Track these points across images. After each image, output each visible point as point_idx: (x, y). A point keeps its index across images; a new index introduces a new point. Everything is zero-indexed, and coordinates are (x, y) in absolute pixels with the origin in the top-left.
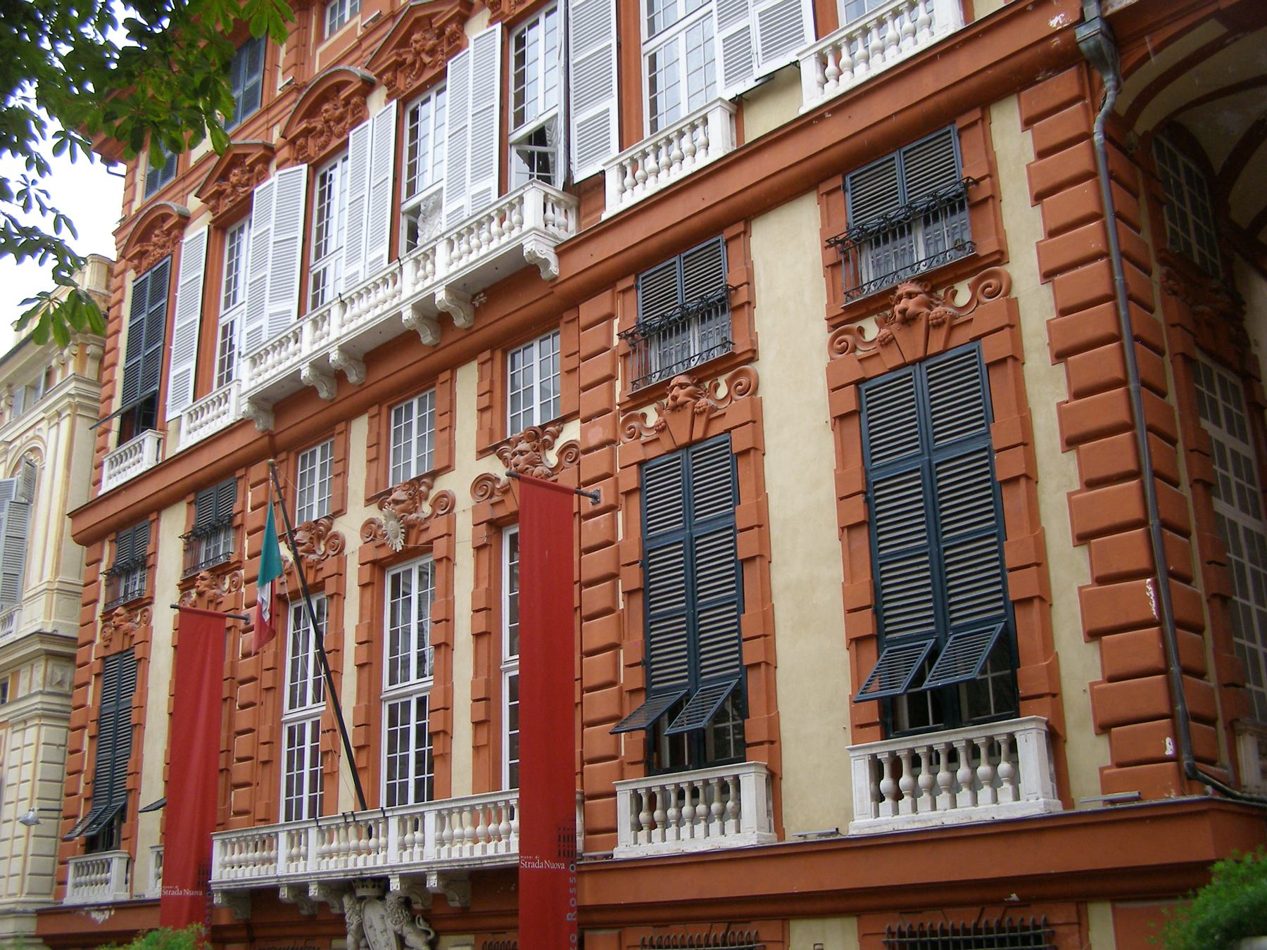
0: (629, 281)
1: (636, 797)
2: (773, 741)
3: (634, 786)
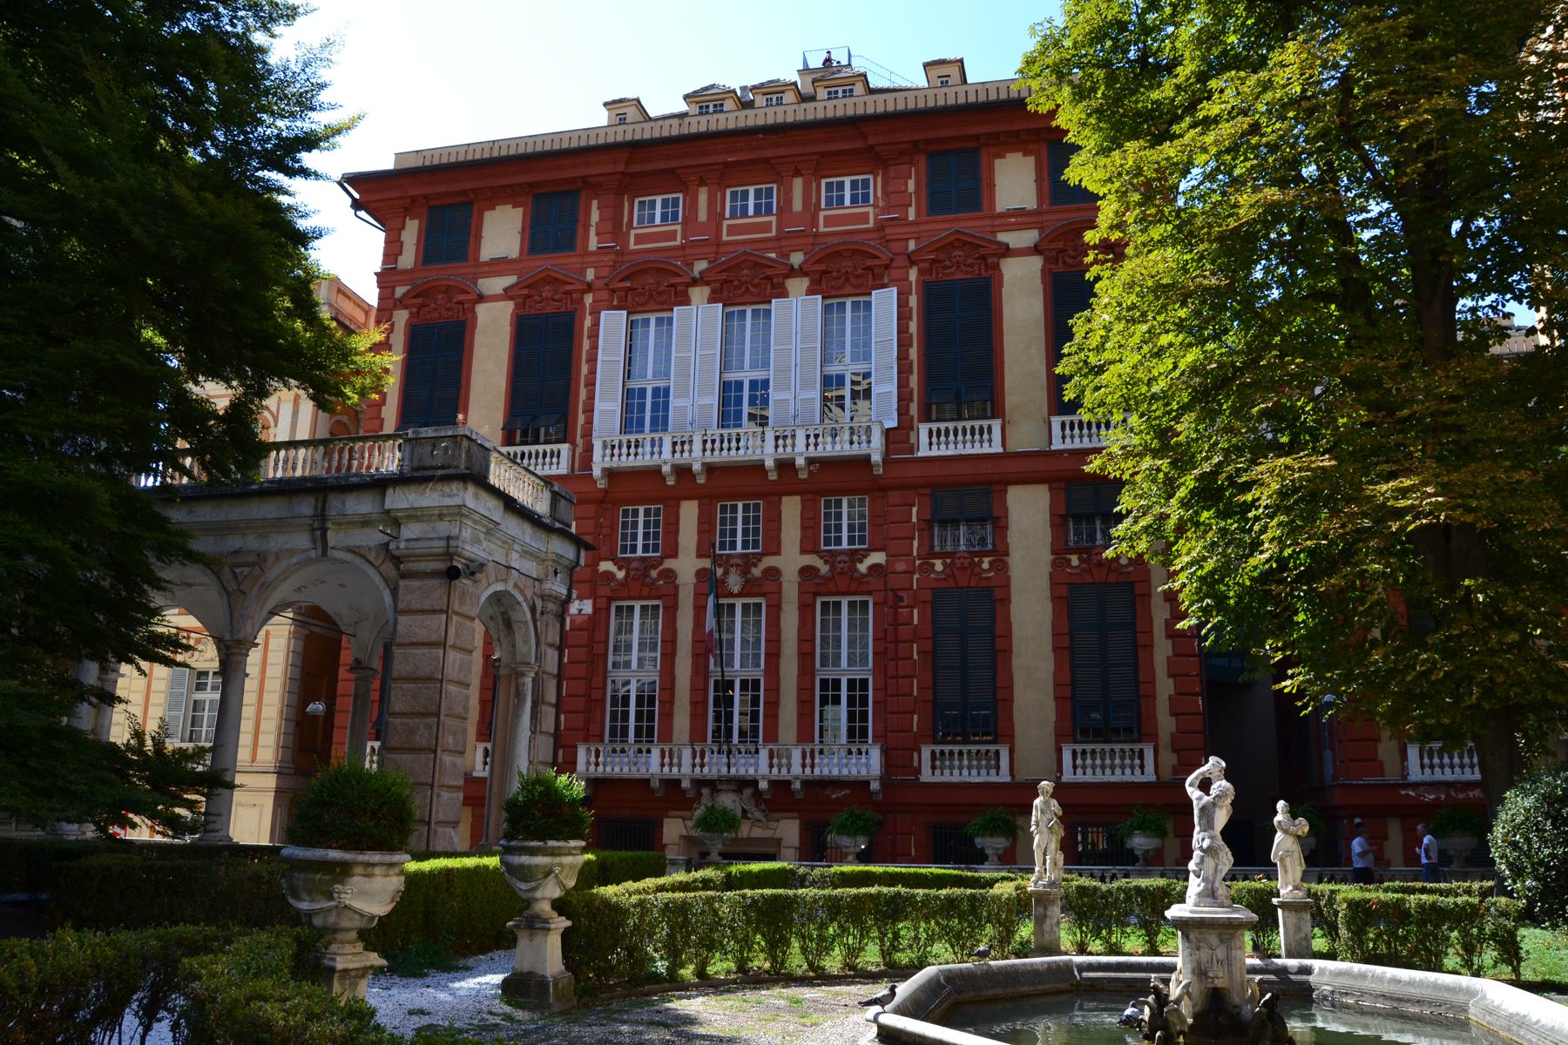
0: (927, 491)
1: (933, 753)
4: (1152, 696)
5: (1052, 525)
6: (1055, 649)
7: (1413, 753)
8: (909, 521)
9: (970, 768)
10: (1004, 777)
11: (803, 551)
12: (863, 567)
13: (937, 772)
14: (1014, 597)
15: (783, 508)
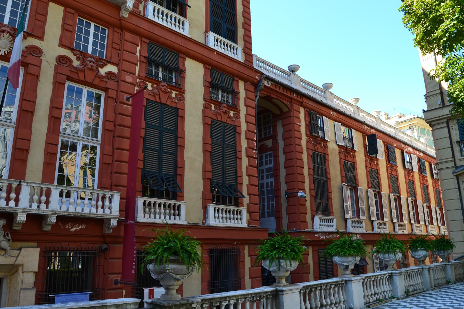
0: (147, 41)
2: (183, 197)
3: (145, 199)
4: (241, 184)
5: (205, 86)
6: (204, 151)
7: (316, 219)
8: (135, 54)
9: (165, 214)
10: (183, 221)
11: (61, 45)
12: (103, 71)
13: (147, 216)
14: (186, 118)
15: (49, 9)
